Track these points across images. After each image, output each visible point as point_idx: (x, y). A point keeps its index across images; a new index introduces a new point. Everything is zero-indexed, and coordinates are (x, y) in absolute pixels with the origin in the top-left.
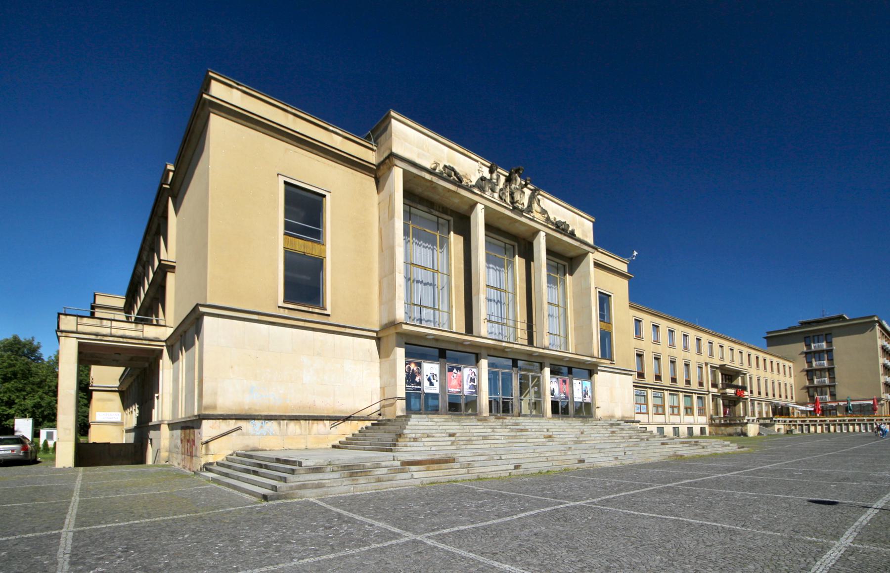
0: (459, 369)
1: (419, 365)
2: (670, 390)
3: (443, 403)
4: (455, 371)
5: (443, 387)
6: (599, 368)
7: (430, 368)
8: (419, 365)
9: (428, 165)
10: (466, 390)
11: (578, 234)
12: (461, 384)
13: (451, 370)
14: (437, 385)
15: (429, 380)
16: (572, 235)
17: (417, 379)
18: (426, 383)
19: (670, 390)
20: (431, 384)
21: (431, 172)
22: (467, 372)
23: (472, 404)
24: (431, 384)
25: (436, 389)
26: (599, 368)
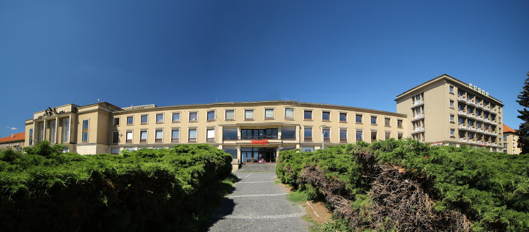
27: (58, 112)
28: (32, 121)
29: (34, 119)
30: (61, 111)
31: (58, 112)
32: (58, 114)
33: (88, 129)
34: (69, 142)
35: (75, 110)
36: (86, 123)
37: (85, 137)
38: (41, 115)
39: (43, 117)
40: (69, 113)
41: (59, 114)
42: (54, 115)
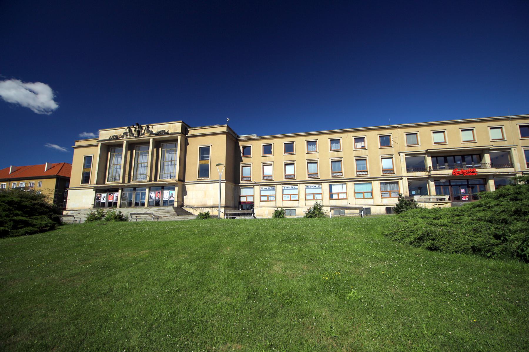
0: (112, 194)
1: (100, 194)
2: (380, 180)
3: (106, 205)
4: (111, 195)
5: (107, 200)
6: (225, 181)
7: (104, 195)
8: (100, 194)
9: (108, 138)
10: (115, 200)
11: (170, 132)
12: (113, 199)
13: (110, 195)
14: (105, 199)
15: (103, 198)
16: (167, 133)
17: (100, 199)
18: (102, 199)
19: (380, 180)
20: (104, 199)
21: (109, 140)
22: (115, 194)
23: (116, 203)
24: (104, 199)
25: (104, 201)
26: (225, 181)
27: (155, 131)
28: (94, 142)
29: (100, 139)
30: (161, 130)
31: (154, 132)
32: (155, 134)
33: (209, 159)
34: (177, 178)
35: (185, 131)
36: (205, 152)
37: (204, 172)
38: (118, 134)
39: (123, 137)
40: (178, 133)
41: (157, 134)
42: (147, 135)
